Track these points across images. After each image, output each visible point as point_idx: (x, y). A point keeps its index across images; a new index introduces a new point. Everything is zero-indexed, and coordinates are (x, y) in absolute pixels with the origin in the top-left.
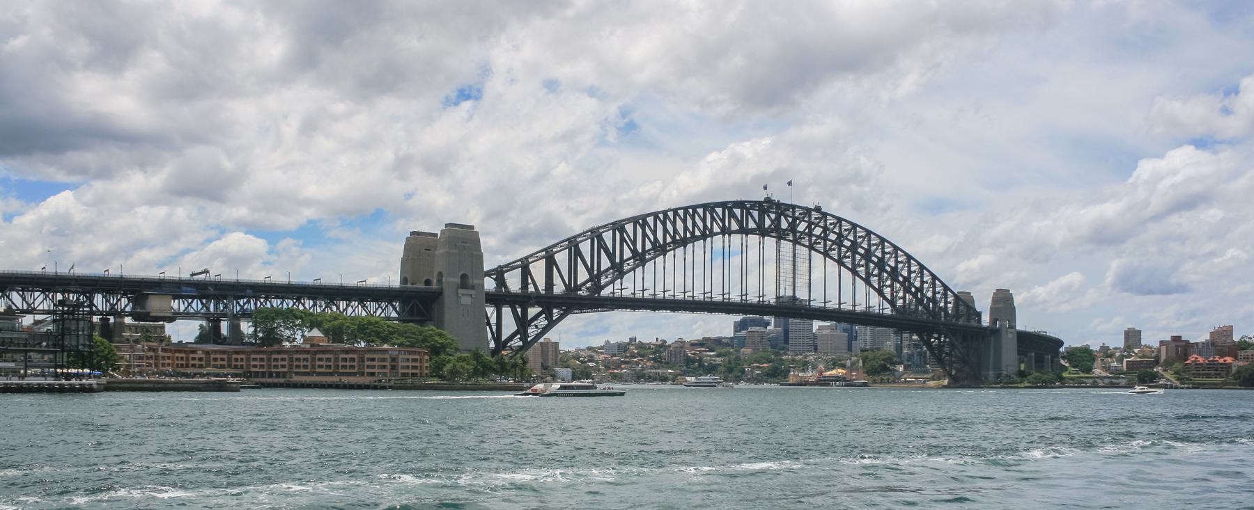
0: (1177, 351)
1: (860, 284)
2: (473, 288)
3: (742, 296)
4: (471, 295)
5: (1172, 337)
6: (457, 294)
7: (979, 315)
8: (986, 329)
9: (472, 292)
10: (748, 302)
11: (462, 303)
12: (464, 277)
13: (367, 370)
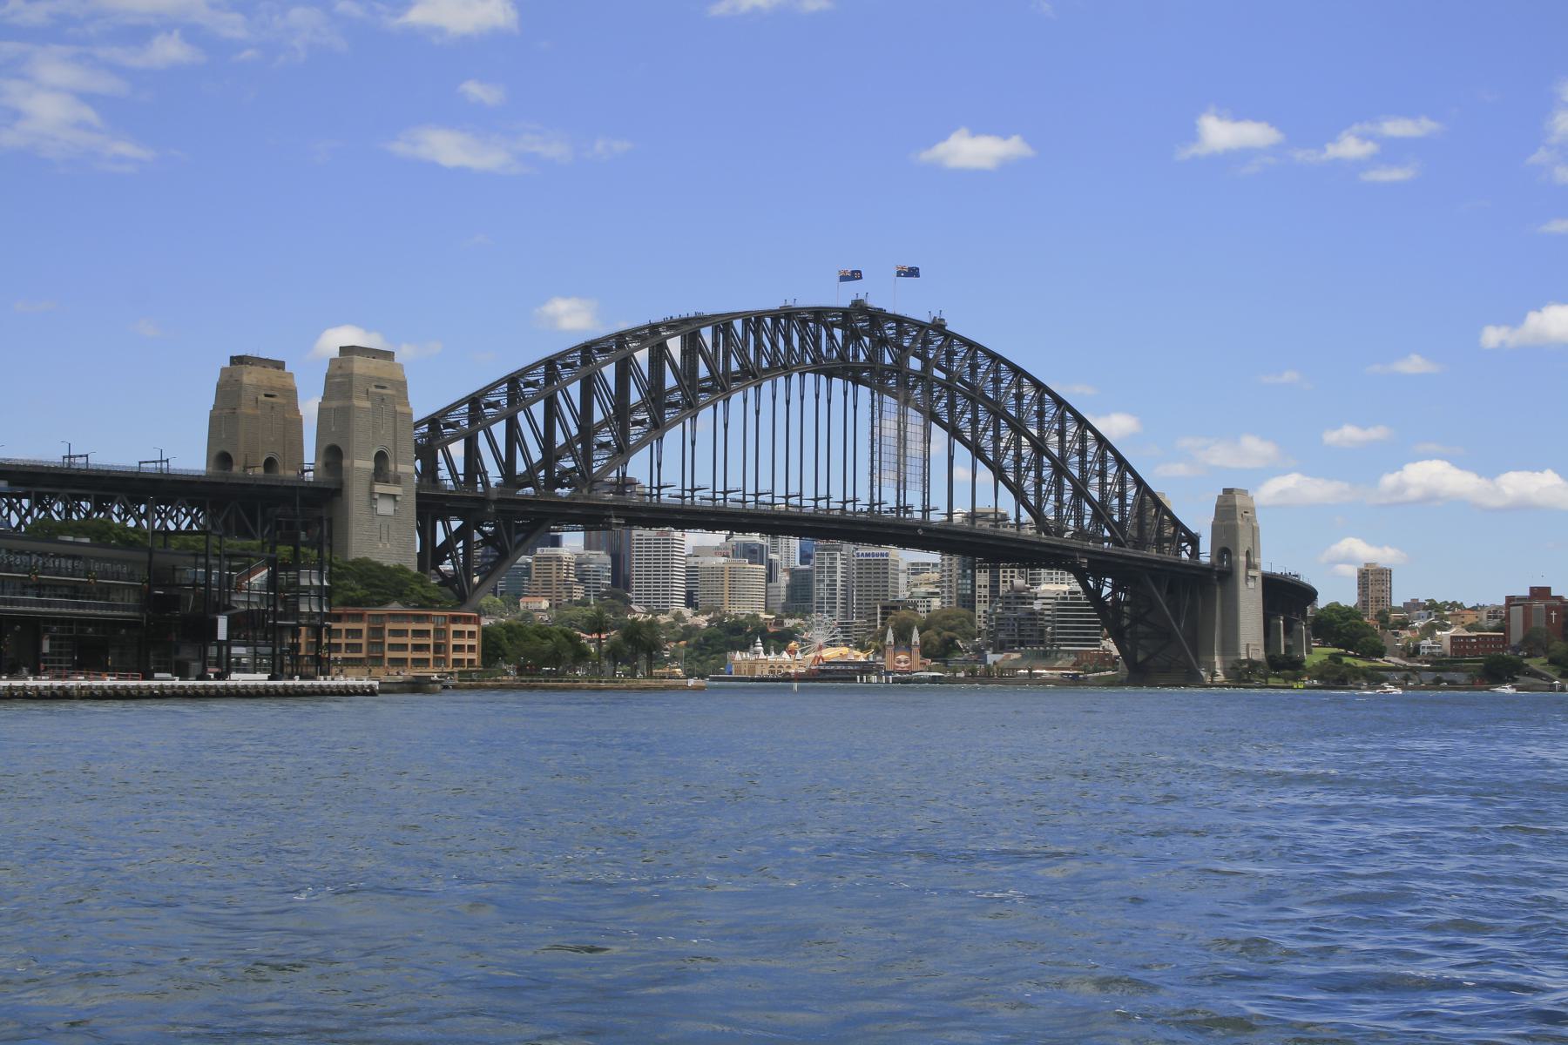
0: (1549, 617)
1: (985, 475)
2: (397, 480)
3: (845, 502)
4: (394, 496)
5: (1532, 589)
6: (372, 493)
7: (1194, 540)
8: (1207, 569)
9: (396, 490)
10: (804, 510)
12: (381, 457)
13: (389, 654)
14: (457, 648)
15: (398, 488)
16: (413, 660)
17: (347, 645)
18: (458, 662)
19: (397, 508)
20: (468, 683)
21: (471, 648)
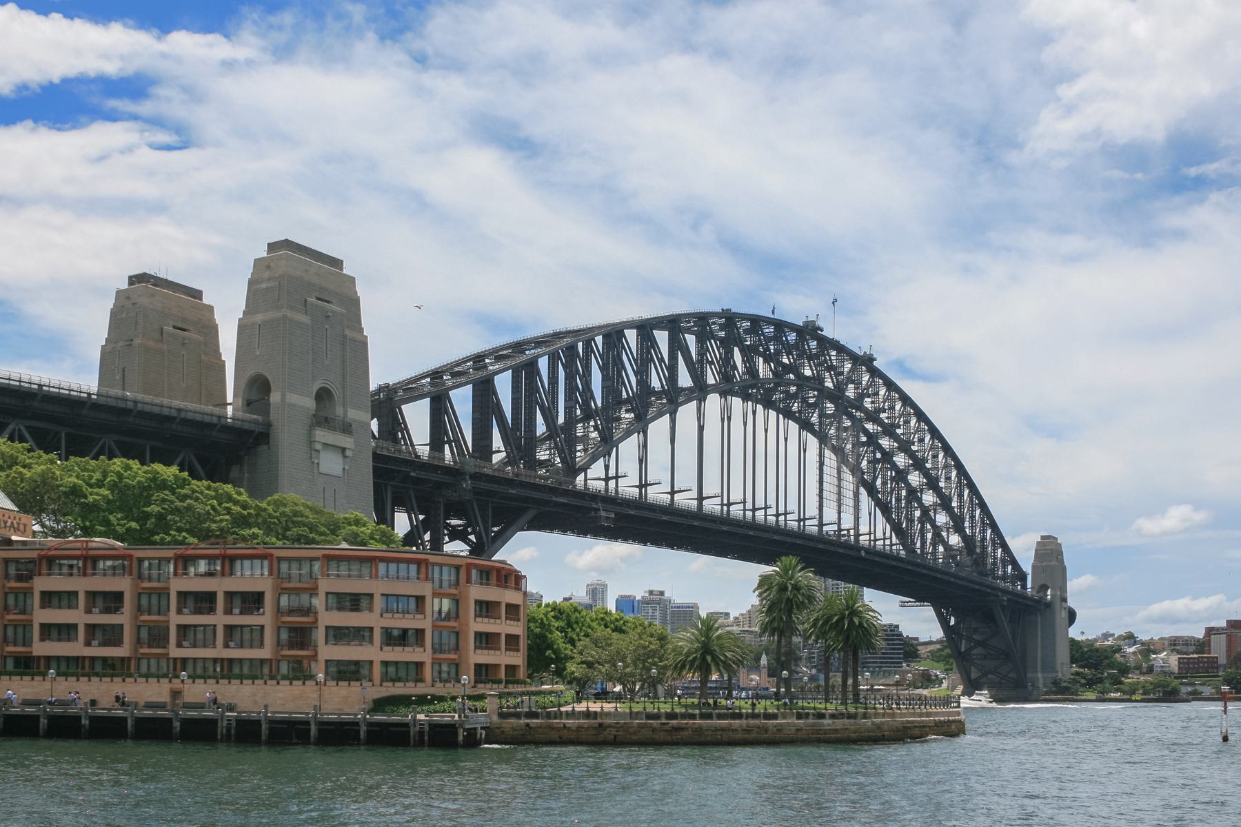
2: (347, 428)
4: (343, 450)
6: (311, 442)
7: (1022, 577)
8: (1031, 599)
9: (346, 441)
11: (322, 470)
12: (323, 396)
14: (486, 640)
15: (348, 439)
16: (385, 664)
17: (230, 629)
18: (484, 673)
19: (347, 467)
20: (523, 721)
21: (512, 641)
